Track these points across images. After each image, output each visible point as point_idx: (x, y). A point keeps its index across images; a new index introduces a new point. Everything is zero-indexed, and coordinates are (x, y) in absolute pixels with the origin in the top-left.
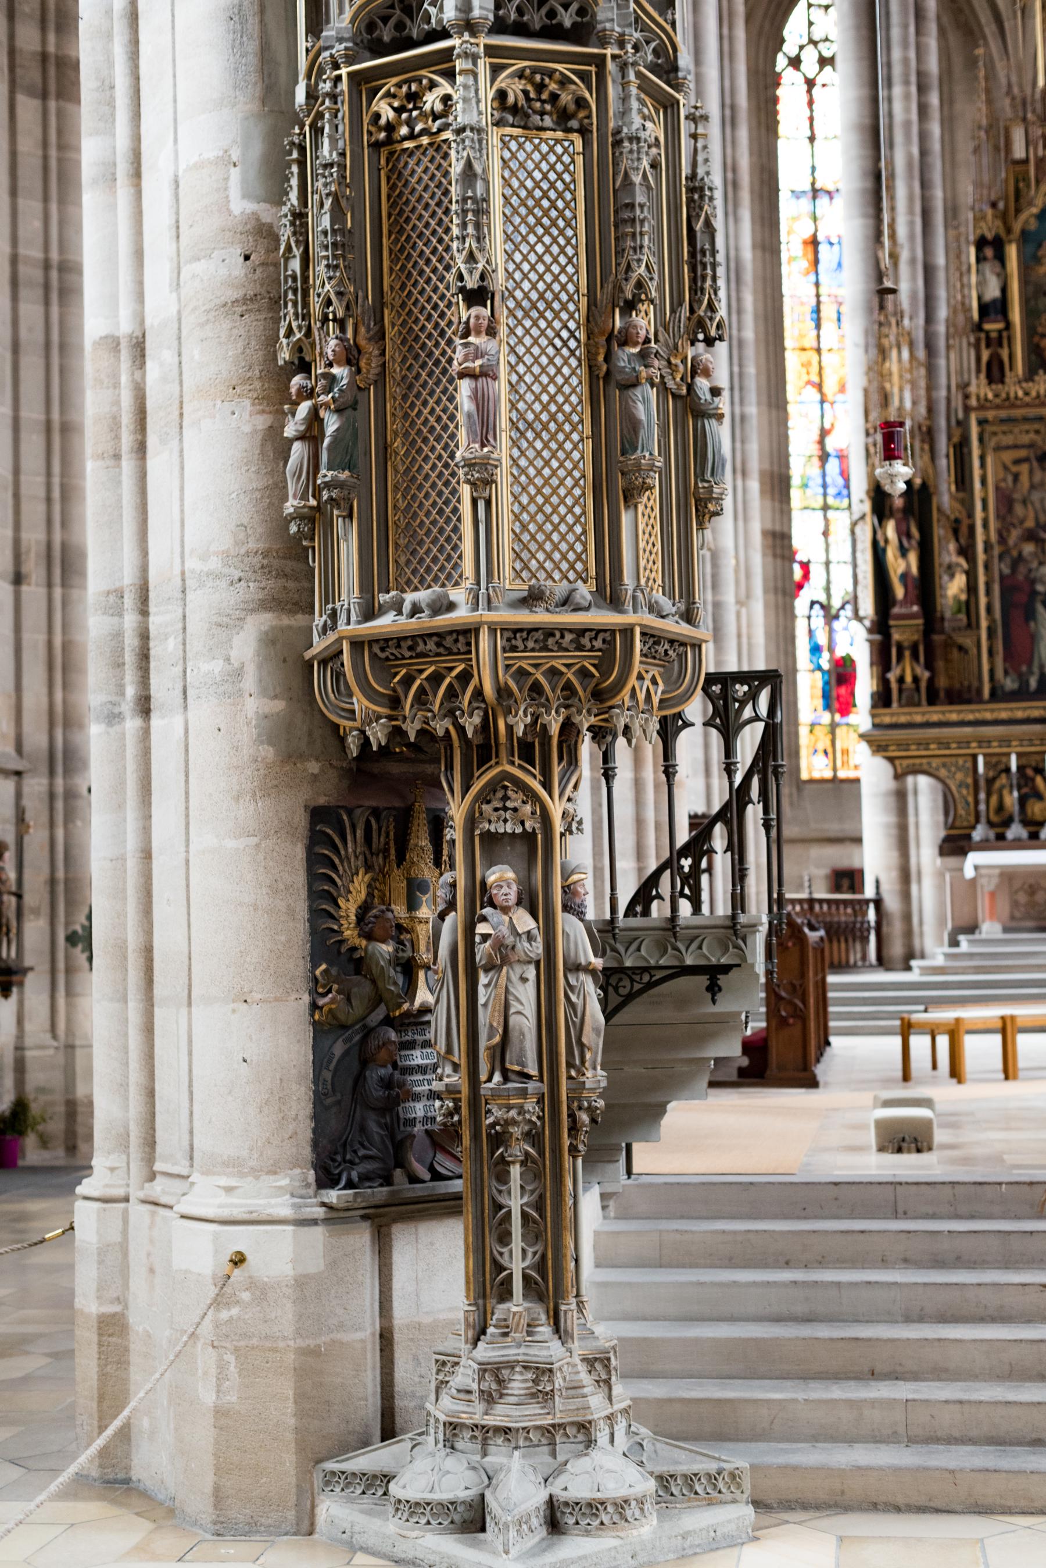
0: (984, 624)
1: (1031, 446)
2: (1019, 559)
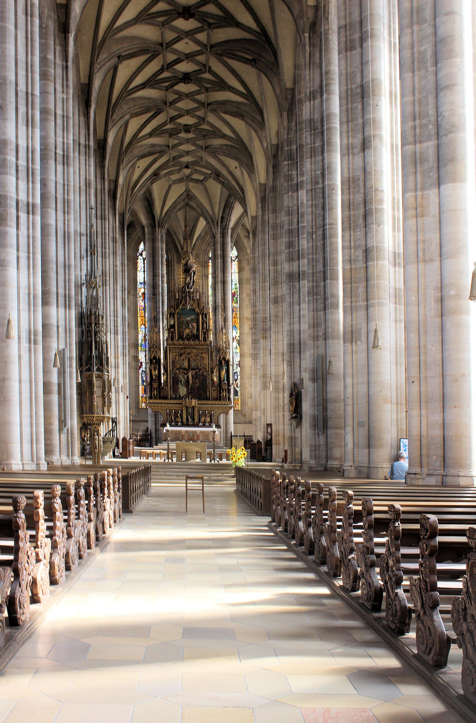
0: (169, 385)
1: (178, 352)
2: (176, 374)
